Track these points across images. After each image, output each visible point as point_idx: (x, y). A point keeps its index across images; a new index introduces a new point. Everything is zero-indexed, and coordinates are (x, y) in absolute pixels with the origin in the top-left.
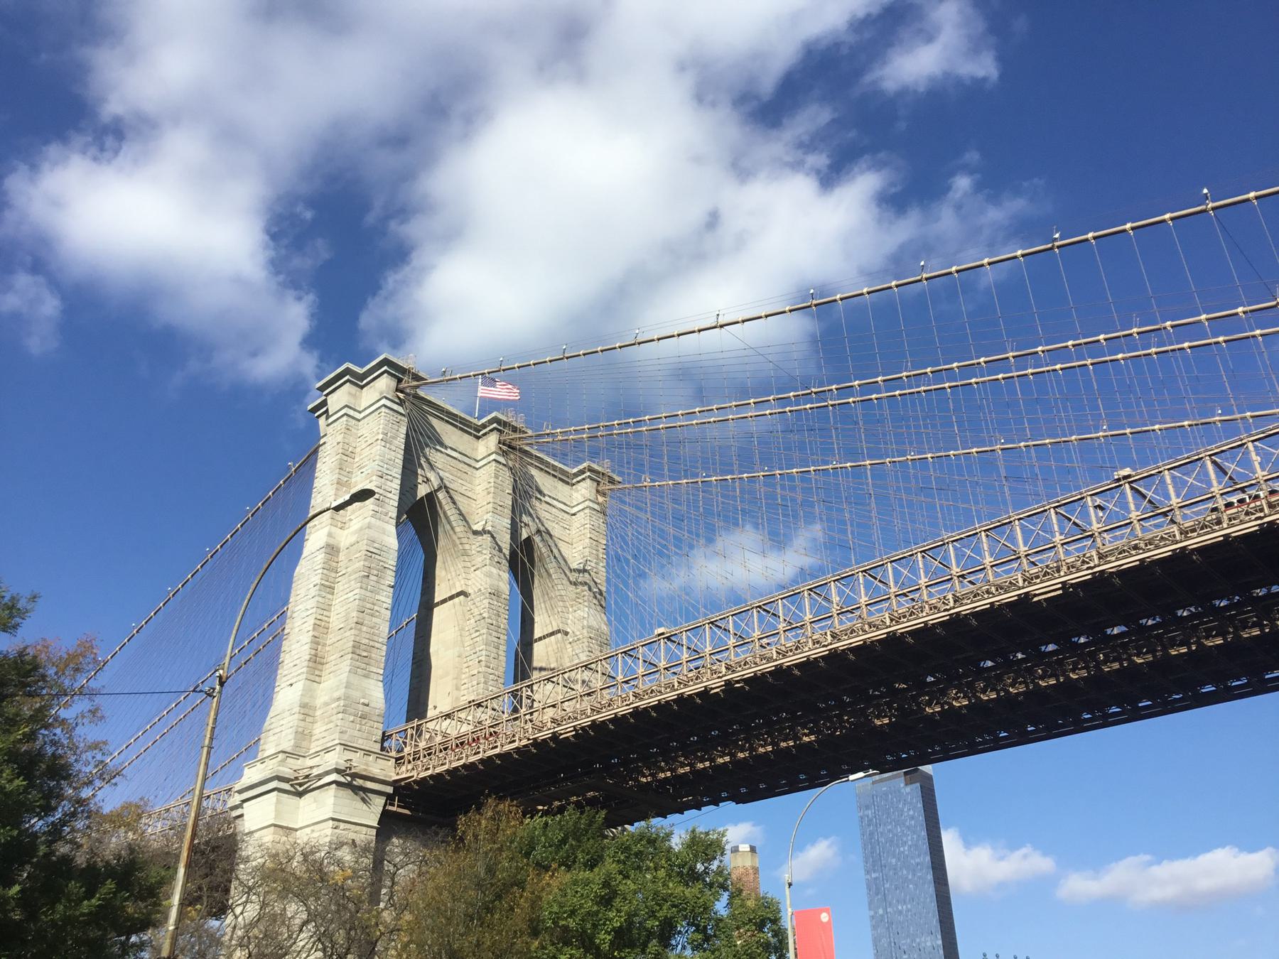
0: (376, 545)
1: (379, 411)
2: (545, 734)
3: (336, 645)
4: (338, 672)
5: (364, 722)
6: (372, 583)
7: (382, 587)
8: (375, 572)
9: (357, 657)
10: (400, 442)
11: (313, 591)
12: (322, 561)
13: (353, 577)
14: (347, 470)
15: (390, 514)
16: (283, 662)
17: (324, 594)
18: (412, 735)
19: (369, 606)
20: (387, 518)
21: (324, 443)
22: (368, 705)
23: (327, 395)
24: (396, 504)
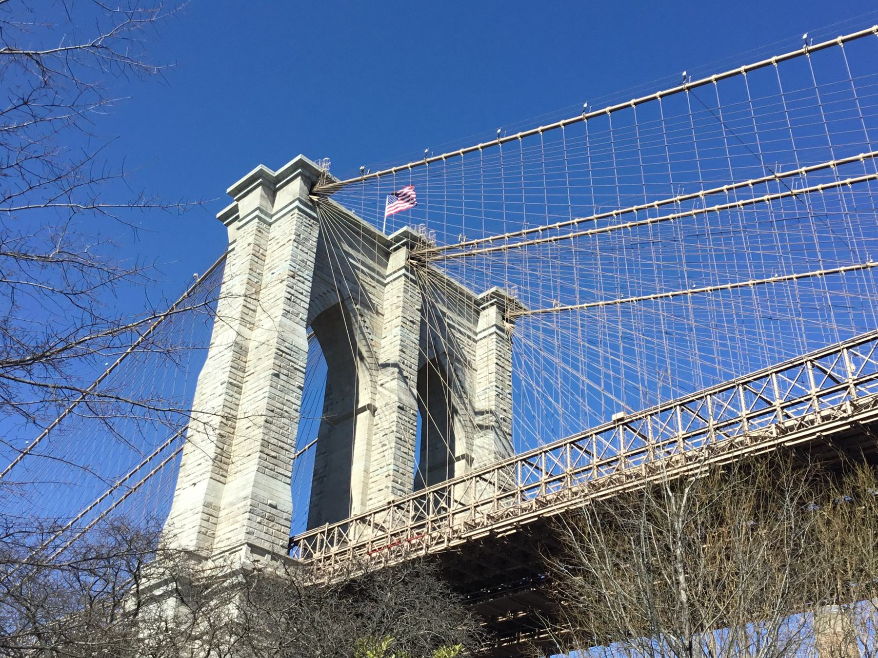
0: (286, 344)
1: (292, 213)
2: (479, 534)
3: (243, 444)
4: (245, 472)
5: (271, 524)
6: (282, 382)
7: (291, 387)
8: (286, 372)
9: (265, 456)
10: (313, 243)
11: (222, 389)
12: (230, 359)
13: (262, 376)
14: (258, 271)
15: (301, 315)
16: (184, 465)
17: (231, 393)
18: (322, 540)
19: (278, 405)
20: (298, 319)
21: (233, 249)
22: (275, 507)
23: (238, 200)
24: (307, 306)
